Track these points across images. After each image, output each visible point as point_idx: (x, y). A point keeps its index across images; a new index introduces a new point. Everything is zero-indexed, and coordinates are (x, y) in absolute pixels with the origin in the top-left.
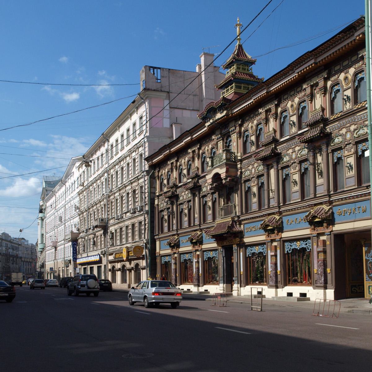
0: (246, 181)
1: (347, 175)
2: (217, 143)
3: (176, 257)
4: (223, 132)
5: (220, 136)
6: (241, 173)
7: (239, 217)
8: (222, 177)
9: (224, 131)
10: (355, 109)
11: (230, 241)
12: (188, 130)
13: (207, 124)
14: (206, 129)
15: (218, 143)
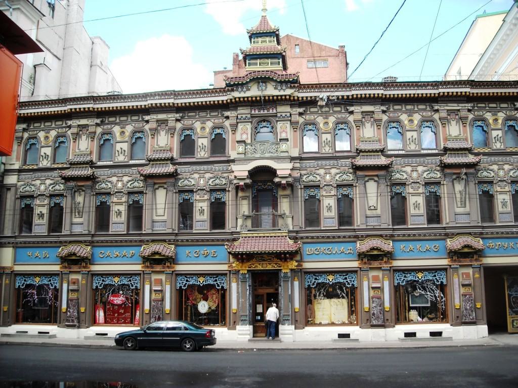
0: (307, 187)
1: (500, 210)
2: (238, 123)
3: (78, 279)
4: (253, 112)
5: (249, 116)
6: (301, 174)
7: (297, 232)
8: (278, 172)
9: (257, 112)
10: (508, 151)
11: (274, 265)
12: (176, 90)
13: (236, 94)
14: (225, 98)
15: (239, 124)
